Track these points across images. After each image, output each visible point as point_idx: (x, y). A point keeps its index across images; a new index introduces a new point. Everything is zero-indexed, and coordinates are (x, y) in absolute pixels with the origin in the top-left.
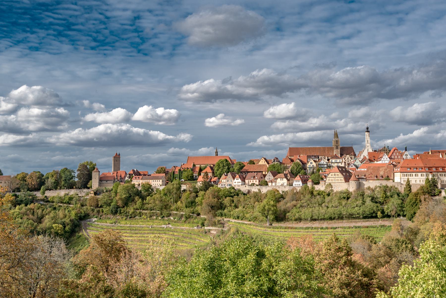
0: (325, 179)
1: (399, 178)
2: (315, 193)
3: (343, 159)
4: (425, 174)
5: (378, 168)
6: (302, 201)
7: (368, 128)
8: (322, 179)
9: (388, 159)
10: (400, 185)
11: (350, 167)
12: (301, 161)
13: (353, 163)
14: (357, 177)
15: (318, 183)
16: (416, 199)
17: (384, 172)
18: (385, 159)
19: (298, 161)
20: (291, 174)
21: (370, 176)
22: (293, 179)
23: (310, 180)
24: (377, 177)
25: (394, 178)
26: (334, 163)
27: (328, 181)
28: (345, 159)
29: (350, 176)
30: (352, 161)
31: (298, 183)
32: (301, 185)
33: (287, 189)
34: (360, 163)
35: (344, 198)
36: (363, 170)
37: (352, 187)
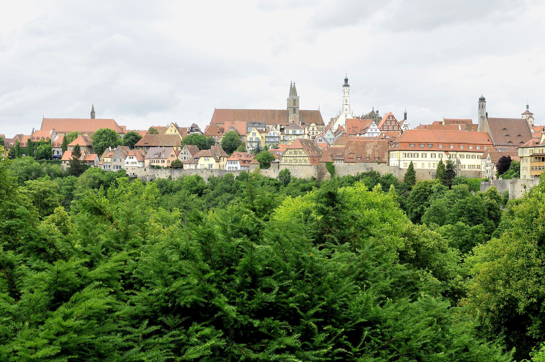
7: (346, 80)
9: (379, 131)
18: (374, 130)
34: (332, 136)
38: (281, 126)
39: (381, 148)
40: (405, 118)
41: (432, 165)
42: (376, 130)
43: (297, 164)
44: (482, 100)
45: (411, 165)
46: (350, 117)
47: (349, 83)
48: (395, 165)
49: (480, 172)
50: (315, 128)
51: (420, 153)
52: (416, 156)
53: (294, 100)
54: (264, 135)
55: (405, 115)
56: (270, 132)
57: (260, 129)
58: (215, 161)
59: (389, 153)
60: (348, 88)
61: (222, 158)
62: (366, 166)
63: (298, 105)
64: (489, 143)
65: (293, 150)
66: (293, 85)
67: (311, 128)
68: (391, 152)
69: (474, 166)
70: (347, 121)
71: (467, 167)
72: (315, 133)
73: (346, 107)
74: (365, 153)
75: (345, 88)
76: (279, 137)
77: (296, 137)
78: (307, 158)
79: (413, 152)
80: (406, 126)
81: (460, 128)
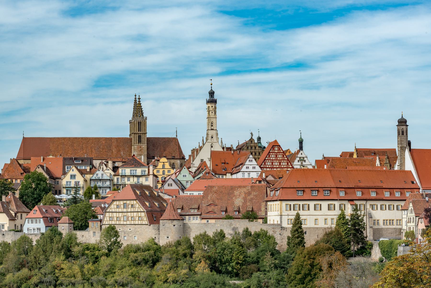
0: (100, 217)
1: (278, 215)
2: (76, 250)
3: (151, 168)
4: (337, 204)
5: (230, 190)
6: (43, 271)
8: (95, 217)
9: (258, 169)
10: (278, 231)
11: (166, 187)
12: (48, 171)
13: (174, 177)
14: (179, 211)
15: (84, 227)
16: (312, 266)
17: (245, 199)
18: (251, 167)
19: (40, 170)
20: (20, 203)
21: (210, 209)
22: (24, 215)
23: (65, 219)
24: (226, 211)
25: (266, 214)
26: (129, 177)
27: (108, 220)
28: (155, 166)
29: (162, 210)
30: (173, 171)
31: (34, 226)
32: (43, 230)
33: (10, 239)
34: (190, 178)
35: (146, 262)
36: (196, 193)
37: (167, 235)
38: (114, 162)
39: (256, 196)
41: (329, 222)
42: (254, 168)
43: (128, 223)
44: (402, 122)
45: (298, 222)
46: (218, 148)
47: (215, 97)
48: (276, 223)
49: (401, 229)
50: (167, 166)
53: (139, 123)
54: (88, 177)
55: (301, 142)
56: (98, 172)
57: (83, 168)
58: (7, 219)
60: (213, 105)
61: (19, 215)
62: (231, 225)
63: (145, 130)
64: (413, 186)
65: (122, 203)
66: (138, 100)
67: (160, 165)
68: (269, 203)
69: (391, 222)
70: (213, 154)
71: (381, 223)
72: (166, 173)
73: (211, 133)
74: (233, 203)
75: (210, 105)
76: (111, 180)
77: (136, 179)
79: (301, 203)
81: (378, 163)
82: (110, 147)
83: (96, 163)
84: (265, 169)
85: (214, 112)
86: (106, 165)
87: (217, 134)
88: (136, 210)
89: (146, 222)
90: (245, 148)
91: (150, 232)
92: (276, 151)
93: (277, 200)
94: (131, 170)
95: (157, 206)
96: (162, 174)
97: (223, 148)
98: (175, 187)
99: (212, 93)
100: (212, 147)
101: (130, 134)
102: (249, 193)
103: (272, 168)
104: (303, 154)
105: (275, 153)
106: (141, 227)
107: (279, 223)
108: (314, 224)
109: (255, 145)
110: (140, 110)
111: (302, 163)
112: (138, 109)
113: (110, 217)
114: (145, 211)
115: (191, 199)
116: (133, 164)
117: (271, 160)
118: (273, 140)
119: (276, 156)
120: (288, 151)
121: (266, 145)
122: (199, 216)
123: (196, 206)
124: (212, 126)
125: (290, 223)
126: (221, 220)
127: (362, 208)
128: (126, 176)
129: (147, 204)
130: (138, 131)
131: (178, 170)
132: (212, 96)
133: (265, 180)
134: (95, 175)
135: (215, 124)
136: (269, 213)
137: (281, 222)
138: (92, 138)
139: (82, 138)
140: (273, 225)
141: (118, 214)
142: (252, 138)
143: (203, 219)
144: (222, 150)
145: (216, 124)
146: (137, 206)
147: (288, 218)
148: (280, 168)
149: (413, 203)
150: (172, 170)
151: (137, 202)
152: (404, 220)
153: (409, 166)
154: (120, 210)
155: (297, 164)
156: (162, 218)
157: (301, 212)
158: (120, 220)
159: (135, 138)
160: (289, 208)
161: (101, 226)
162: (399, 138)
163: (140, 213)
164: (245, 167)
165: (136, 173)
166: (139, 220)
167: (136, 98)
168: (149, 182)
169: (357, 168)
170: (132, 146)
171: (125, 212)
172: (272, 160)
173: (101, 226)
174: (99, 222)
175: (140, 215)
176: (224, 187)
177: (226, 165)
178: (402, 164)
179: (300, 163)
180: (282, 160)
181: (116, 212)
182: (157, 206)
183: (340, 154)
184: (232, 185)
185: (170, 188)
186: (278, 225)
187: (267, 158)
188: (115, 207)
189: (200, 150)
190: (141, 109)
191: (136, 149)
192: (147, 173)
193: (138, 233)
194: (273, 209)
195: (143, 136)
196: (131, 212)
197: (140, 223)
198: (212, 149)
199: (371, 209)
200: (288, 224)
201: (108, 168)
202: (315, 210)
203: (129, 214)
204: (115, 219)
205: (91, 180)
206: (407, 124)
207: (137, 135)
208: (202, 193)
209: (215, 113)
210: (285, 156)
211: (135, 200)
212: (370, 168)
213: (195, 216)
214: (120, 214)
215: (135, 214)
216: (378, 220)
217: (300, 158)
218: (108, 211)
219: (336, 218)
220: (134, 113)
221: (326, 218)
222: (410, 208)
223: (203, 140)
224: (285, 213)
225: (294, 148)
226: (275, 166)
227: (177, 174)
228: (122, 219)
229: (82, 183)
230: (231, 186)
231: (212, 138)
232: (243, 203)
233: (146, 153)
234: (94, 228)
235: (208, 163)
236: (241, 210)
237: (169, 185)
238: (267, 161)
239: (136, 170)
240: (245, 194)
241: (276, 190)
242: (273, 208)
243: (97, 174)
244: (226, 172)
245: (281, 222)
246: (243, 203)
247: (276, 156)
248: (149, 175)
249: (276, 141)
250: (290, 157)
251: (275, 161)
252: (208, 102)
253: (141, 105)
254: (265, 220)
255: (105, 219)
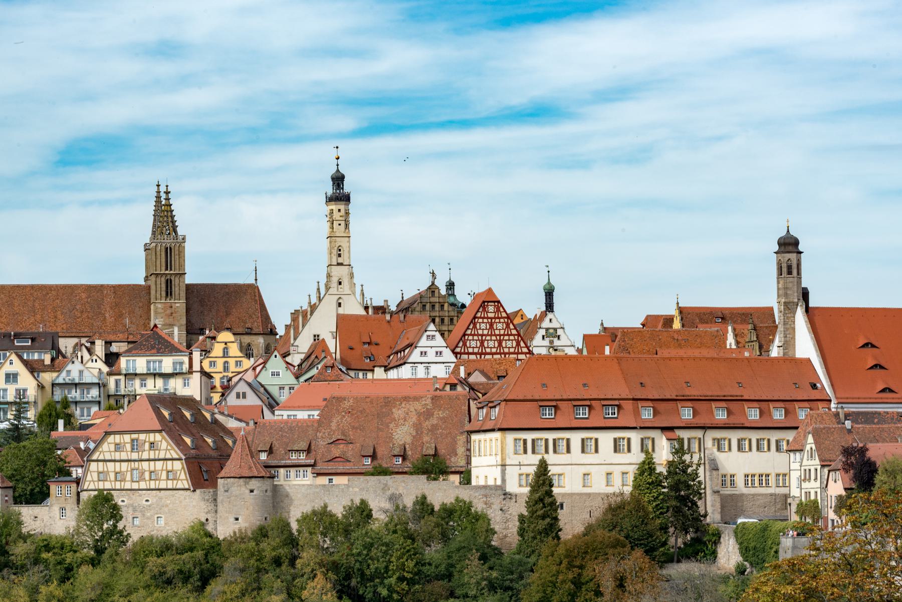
0: (77, 472)
3: (196, 355)
4: (635, 437)
5: (384, 406)
9: (448, 356)
11: (232, 400)
13: (249, 377)
14: (263, 456)
15: (39, 496)
16: (578, 583)
17: (418, 427)
18: (431, 353)
21: (336, 451)
24: (374, 457)
25: (469, 462)
26: (143, 377)
27: (93, 480)
28: (206, 352)
29: (223, 455)
30: (247, 363)
34: (288, 378)
35: (186, 577)
36: (302, 415)
37: (233, 513)
38: (108, 343)
40: (550, 307)
41: (617, 480)
43: (143, 485)
44: (789, 245)
45: (542, 480)
46: (353, 308)
47: (347, 187)
48: (491, 482)
49: (786, 496)
50: (234, 350)
51: (576, 438)
52: (563, 446)
53: (168, 251)
54: (47, 377)
55: (549, 294)
56: (70, 367)
59: (468, 441)
60: (342, 207)
62: (385, 488)
63: (182, 266)
64: (814, 395)
65: (127, 438)
66: (163, 196)
67: (218, 350)
68: (474, 437)
69: (763, 478)
70: (343, 322)
71: (740, 481)
72: (232, 367)
73: (337, 272)
75: (334, 207)
76: (102, 386)
77: (160, 382)
78: (178, 465)
79: (551, 436)
80: (553, 334)
81: (731, 341)
82: (99, 308)
83: (66, 344)
84: (465, 357)
85: (343, 223)
86: (88, 350)
87: (352, 276)
88: (162, 456)
89: (185, 482)
90: (418, 309)
91: (194, 506)
92: (490, 315)
93: (493, 430)
94: (148, 362)
95: (211, 444)
96: (222, 370)
97: (366, 308)
98: (252, 400)
99: (338, 180)
100: (340, 305)
101: (147, 277)
102: (428, 414)
103: (481, 354)
104: (554, 320)
105: (488, 318)
106: (173, 496)
107: (499, 483)
108: (581, 485)
109: (441, 300)
110: (170, 219)
111: (551, 342)
112: (164, 218)
113: (99, 473)
114: (184, 457)
115: (291, 429)
116: (153, 348)
117: (478, 335)
118: (482, 289)
119: (491, 325)
120: (519, 314)
121: (467, 301)
122: (309, 469)
123: (304, 445)
124: (340, 255)
125: (524, 482)
126: (362, 478)
127: (695, 446)
128: (136, 375)
129: (188, 440)
130: (164, 268)
131: (261, 361)
132: (338, 185)
133: (464, 382)
134: (64, 374)
135: (346, 250)
136: (475, 461)
137: (504, 480)
138: (57, 286)
139: (32, 287)
140: (485, 487)
141: (118, 464)
142: (433, 283)
143: (319, 474)
144: (363, 313)
145: (349, 252)
146: (164, 445)
147: (521, 472)
148: (500, 353)
149: (816, 434)
150: (245, 360)
151: (163, 438)
152: (795, 476)
153: (805, 347)
154: (124, 456)
155: (539, 345)
156: (222, 474)
157: (551, 458)
158: (124, 480)
159: (158, 286)
160: (522, 448)
161: (78, 494)
162: (781, 282)
163: (169, 463)
164: (417, 351)
165: (160, 367)
166: (168, 479)
167: (159, 192)
168: (192, 388)
169: (681, 353)
170: (149, 303)
171: (135, 461)
172: (482, 335)
173: (78, 494)
174: (75, 485)
175: (170, 468)
176: (368, 400)
177: (373, 349)
178: (789, 344)
179: (546, 342)
180: (504, 335)
181: (114, 461)
182: (211, 444)
183: (642, 320)
184: (387, 395)
185: (241, 402)
186: (496, 487)
187: (469, 332)
188: (112, 447)
189: (312, 313)
190: (173, 217)
191: (160, 310)
192: (186, 367)
193: (166, 509)
194: (485, 451)
195: (175, 281)
196: (149, 460)
197: (170, 486)
198: (341, 311)
199: (715, 450)
200: (520, 486)
201: (95, 358)
202: (583, 451)
203: (145, 465)
204: (112, 476)
205: (53, 385)
206: (801, 248)
207: (163, 280)
208: (316, 413)
209: (347, 226)
210: (511, 326)
211: (160, 431)
212: (712, 353)
213: (301, 469)
214: (124, 465)
215: (159, 464)
216: (732, 476)
217: (547, 329)
218: (95, 457)
219: (632, 470)
220: (154, 226)
221: (609, 471)
222: (808, 447)
223: (318, 289)
224: (512, 459)
225: (533, 307)
226: (488, 350)
227: (258, 369)
228: (128, 478)
229: (32, 392)
230: (385, 398)
231: (340, 283)
232: (414, 437)
233: (184, 321)
234: (63, 499)
235: (331, 344)
236: (409, 453)
237: (238, 396)
238: (471, 338)
239: (160, 362)
240: (419, 414)
241: (490, 405)
242: (485, 447)
243: (69, 372)
244: (373, 363)
245: (504, 480)
246: (414, 437)
247: (491, 325)
248: (190, 371)
249: (490, 291)
250: (524, 329)
251: (488, 338)
252: (330, 200)
253: (173, 207)
254: (466, 477)
255: (89, 478)
